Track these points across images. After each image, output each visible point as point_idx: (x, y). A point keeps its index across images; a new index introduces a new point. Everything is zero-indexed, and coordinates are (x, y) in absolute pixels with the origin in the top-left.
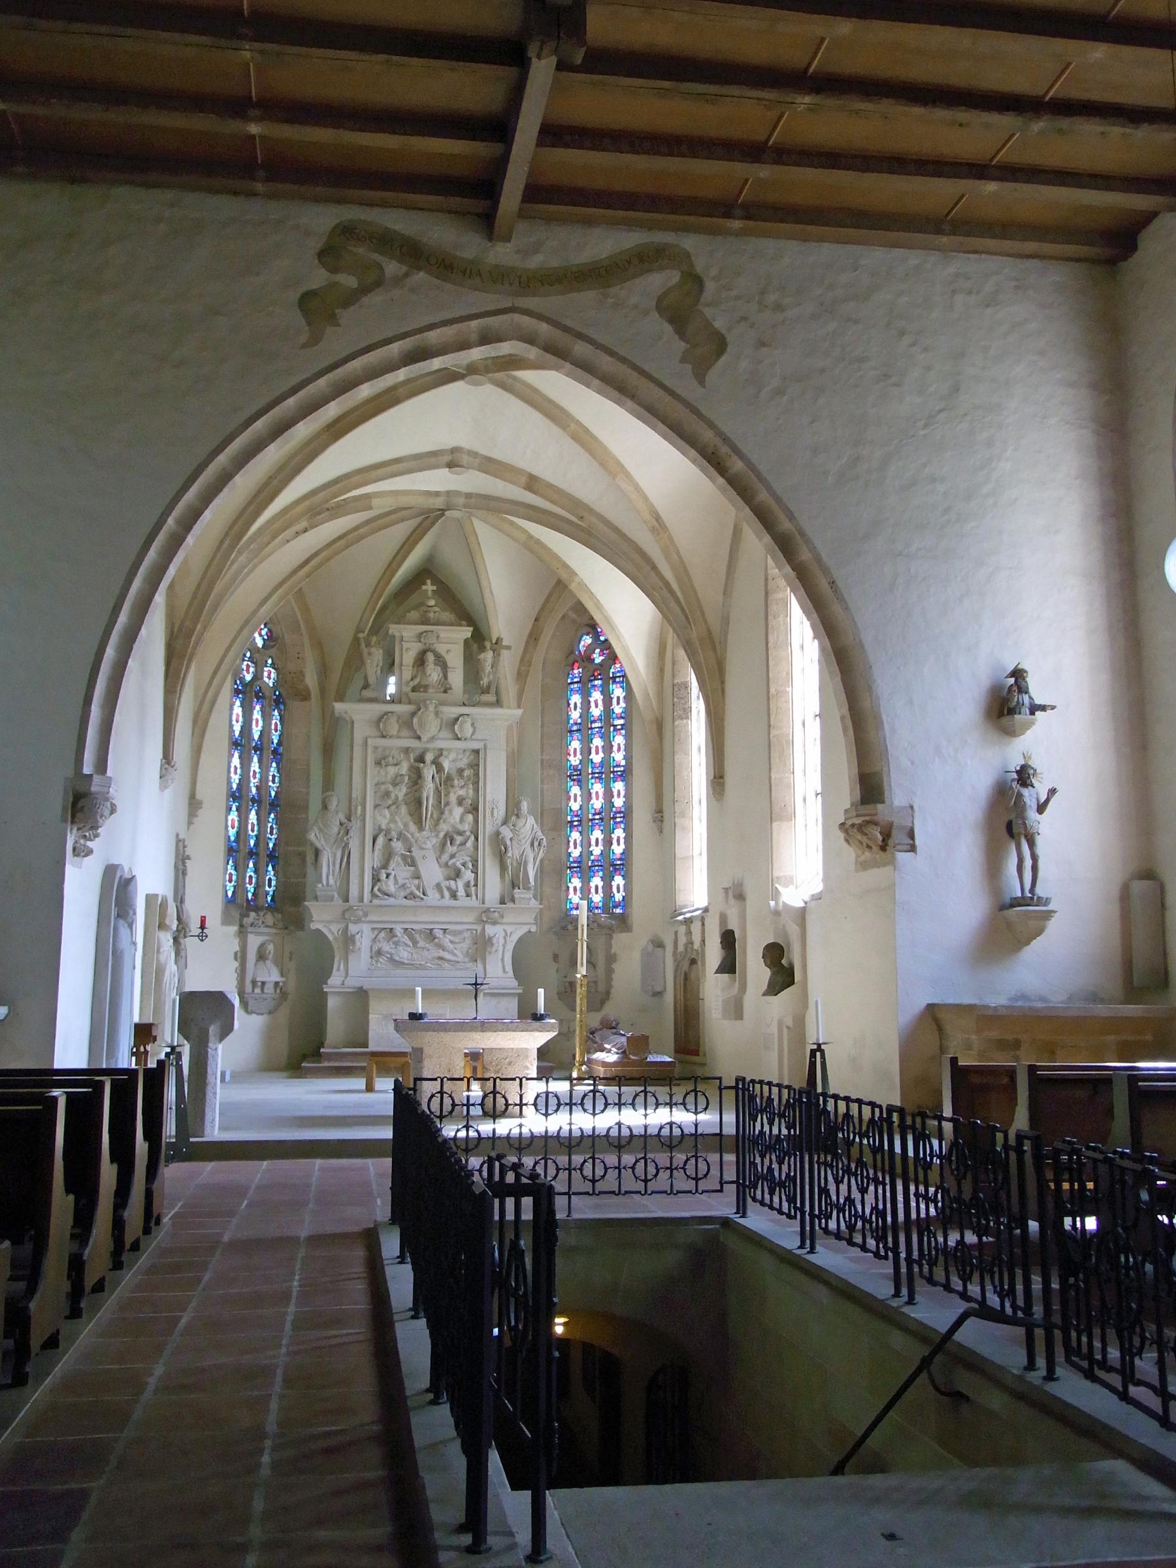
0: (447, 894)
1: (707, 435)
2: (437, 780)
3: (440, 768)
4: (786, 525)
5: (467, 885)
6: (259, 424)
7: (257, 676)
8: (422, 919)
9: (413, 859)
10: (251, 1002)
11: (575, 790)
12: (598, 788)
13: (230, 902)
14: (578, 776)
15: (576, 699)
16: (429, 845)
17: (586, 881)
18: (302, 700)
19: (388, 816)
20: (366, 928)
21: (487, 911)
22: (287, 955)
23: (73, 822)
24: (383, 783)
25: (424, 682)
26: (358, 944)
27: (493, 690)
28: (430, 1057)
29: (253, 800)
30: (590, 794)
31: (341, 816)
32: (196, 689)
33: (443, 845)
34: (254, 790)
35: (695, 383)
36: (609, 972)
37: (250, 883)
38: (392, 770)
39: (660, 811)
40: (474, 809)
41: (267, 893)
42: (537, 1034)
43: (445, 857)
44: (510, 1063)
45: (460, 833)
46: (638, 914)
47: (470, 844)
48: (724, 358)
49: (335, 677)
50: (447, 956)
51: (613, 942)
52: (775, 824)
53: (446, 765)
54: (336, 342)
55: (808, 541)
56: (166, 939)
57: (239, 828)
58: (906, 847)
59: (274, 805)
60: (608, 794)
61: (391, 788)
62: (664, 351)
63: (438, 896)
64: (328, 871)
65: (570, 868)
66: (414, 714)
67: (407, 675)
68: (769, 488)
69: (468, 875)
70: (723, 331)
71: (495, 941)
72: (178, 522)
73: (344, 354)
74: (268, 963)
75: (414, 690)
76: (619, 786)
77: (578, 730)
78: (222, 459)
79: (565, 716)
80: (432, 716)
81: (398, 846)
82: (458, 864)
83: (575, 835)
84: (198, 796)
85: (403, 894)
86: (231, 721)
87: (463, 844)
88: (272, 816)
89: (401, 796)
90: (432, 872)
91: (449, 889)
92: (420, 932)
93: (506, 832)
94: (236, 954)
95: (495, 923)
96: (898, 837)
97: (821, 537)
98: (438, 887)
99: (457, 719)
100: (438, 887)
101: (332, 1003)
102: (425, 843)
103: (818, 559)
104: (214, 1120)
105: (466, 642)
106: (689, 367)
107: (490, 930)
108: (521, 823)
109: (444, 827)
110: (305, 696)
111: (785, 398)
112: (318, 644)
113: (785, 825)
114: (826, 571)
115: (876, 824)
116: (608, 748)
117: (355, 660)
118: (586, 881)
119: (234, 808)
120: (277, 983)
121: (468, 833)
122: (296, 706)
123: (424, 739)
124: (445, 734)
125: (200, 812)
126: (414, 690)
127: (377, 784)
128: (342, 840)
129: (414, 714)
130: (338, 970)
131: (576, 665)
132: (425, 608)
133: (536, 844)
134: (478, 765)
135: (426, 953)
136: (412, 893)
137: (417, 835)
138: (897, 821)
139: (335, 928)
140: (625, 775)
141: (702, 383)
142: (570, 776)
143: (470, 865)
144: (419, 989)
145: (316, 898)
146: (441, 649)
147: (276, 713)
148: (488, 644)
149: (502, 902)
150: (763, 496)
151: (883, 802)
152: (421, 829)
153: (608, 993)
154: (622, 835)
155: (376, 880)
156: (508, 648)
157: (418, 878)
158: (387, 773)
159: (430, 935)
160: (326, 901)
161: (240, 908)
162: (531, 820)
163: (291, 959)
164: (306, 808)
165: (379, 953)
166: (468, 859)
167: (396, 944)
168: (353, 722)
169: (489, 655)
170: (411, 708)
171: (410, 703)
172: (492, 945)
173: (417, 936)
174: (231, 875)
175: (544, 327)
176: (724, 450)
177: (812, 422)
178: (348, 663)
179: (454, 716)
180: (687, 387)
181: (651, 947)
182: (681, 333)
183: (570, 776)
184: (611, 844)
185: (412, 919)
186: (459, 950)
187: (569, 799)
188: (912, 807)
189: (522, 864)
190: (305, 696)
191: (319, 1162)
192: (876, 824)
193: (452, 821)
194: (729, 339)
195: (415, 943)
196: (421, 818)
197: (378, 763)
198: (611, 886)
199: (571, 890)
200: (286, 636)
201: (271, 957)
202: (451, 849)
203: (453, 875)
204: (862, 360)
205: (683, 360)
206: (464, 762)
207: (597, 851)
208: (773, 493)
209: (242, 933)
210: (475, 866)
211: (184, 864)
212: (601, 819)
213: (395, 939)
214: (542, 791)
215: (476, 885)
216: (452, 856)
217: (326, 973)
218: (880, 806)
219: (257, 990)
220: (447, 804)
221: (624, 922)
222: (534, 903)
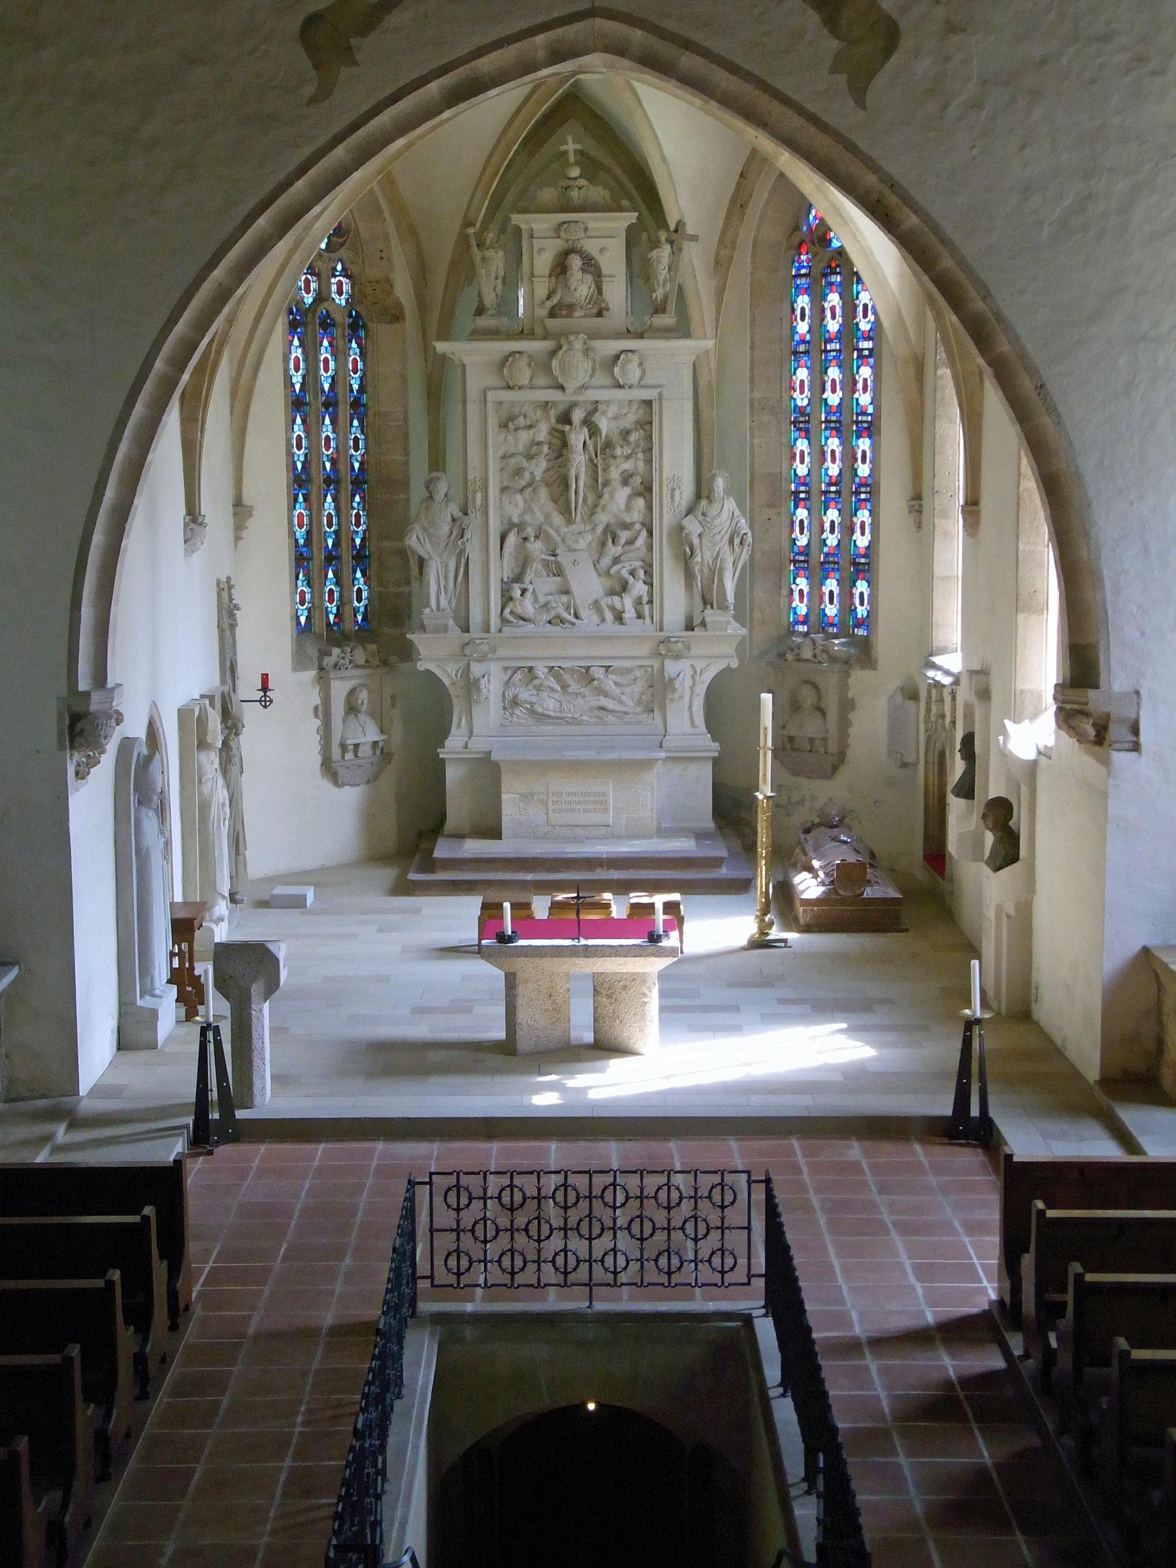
0: (609, 616)
1: (870, 179)
2: (591, 449)
3: (594, 431)
4: (979, 305)
5: (638, 602)
6: (262, 222)
7: (320, 298)
8: (574, 653)
9: (557, 564)
10: (342, 772)
11: (802, 445)
12: (834, 444)
13: (303, 631)
14: (802, 422)
15: (803, 301)
16: (582, 544)
17: (816, 584)
18: (391, 322)
19: (521, 504)
20: (494, 668)
21: (665, 641)
22: (387, 702)
23: (72, 747)
24: (512, 455)
25: (568, 300)
26: (485, 691)
27: (672, 306)
28: (527, 981)
29: (328, 481)
30: (823, 453)
31: (454, 509)
32: (231, 360)
33: (603, 544)
34: (328, 465)
35: (851, 103)
36: (844, 724)
37: (331, 601)
38: (524, 436)
39: (918, 497)
40: (646, 490)
41: (356, 610)
42: (653, 959)
43: (606, 561)
44: (624, 988)
45: (626, 526)
46: (884, 644)
47: (641, 541)
48: (893, 60)
49: (437, 291)
50: (610, 704)
51: (850, 681)
52: (1021, 617)
53: (604, 425)
54: (355, 89)
55: (1009, 330)
56: (210, 761)
57: (310, 524)
58: (1126, 746)
59: (358, 483)
60: (850, 457)
61: (524, 463)
62: (807, 58)
63: (596, 618)
64: (437, 590)
65: (795, 562)
66: (553, 353)
67: (542, 290)
68: (954, 251)
69: (639, 588)
70: (895, 15)
71: (677, 684)
72: (169, 362)
73: (365, 108)
74: (362, 717)
75: (552, 314)
76: (864, 444)
77: (807, 352)
78: (218, 274)
79: (786, 330)
80: (579, 356)
81: (536, 548)
82: (625, 573)
83: (802, 513)
84: (247, 500)
85: (546, 617)
86: (286, 370)
87: (630, 542)
88: (357, 499)
89: (539, 473)
90: (587, 584)
91: (612, 608)
92: (572, 671)
93: (692, 526)
94: (316, 708)
95: (678, 657)
96: (1117, 732)
97: (1028, 323)
98: (596, 605)
99: (617, 357)
100: (596, 605)
101: (452, 774)
102: (576, 541)
103: (1022, 354)
104: (264, 1088)
105: (630, 230)
106: (842, 79)
107: (672, 668)
108: (716, 506)
109: (603, 518)
110: (397, 317)
111: (984, 114)
112: (410, 232)
113: (1034, 619)
114: (1032, 371)
115: (1087, 715)
116: (850, 384)
117: (463, 269)
118: (816, 584)
119: (301, 499)
120: (375, 743)
121: (638, 526)
122: (382, 332)
123: (571, 387)
124: (601, 379)
125: (250, 523)
126: (552, 314)
127: (504, 457)
128: (455, 546)
129: (553, 353)
130: (459, 726)
131: (803, 251)
132: (564, 183)
133: (737, 541)
134: (651, 423)
135: (580, 700)
136: (558, 617)
137: (564, 530)
138: (1115, 713)
139: (451, 668)
140: (870, 430)
141: (861, 103)
142: (794, 423)
143: (641, 573)
144: (507, 905)
145: (423, 628)
146: (591, 246)
147: (354, 345)
148: (663, 236)
149: (690, 627)
150: (947, 262)
151: (1096, 686)
152: (570, 521)
153: (842, 756)
154: (868, 521)
155: (506, 598)
156: (694, 238)
157: (567, 592)
158: (517, 440)
159: (586, 676)
160: (437, 631)
161: (321, 639)
162: (731, 505)
163: (393, 706)
164: (405, 484)
165: (515, 702)
166: (638, 564)
167: (538, 689)
168: (464, 366)
169: (664, 253)
170: (548, 345)
171: (545, 338)
172: (674, 690)
173: (567, 677)
174: (303, 593)
175: (637, 35)
176: (892, 199)
177: (1023, 148)
178: (454, 265)
179: (613, 352)
180: (841, 113)
181: (899, 699)
182: (832, 23)
183: (794, 423)
184: (852, 532)
185: (558, 652)
186: (627, 695)
187: (793, 457)
188: (1137, 693)
189: (715, 572)
190: (397, 317)
191: (380, 1146)
192: (1087, 715)
193: (615, 509)
194: (902, 25)
195: (565, 687)
196: (569, 506)
197: (504, 426)
198: (852, 595)
199: (796, 595)
200: (361, 226)
201: (364, 708)
202: (612, 551)
203: (618, 588)
204: (1105, 38)
205: (834, 70)
206: (632, 416)
207: (832, 540)
208: (961, 261)
209: (323, 679)
210: (649, 573)
211: (232, 615)
212: (838, 492)
213: (536, 682)
214: (752, 448)
215: (650, 602)
216: (616, 560)
217: (442, 732)
218: (1092, 693)
219: (349, 756)
220: (606, 483)
221: (865, 653)
222: (735, 630)
